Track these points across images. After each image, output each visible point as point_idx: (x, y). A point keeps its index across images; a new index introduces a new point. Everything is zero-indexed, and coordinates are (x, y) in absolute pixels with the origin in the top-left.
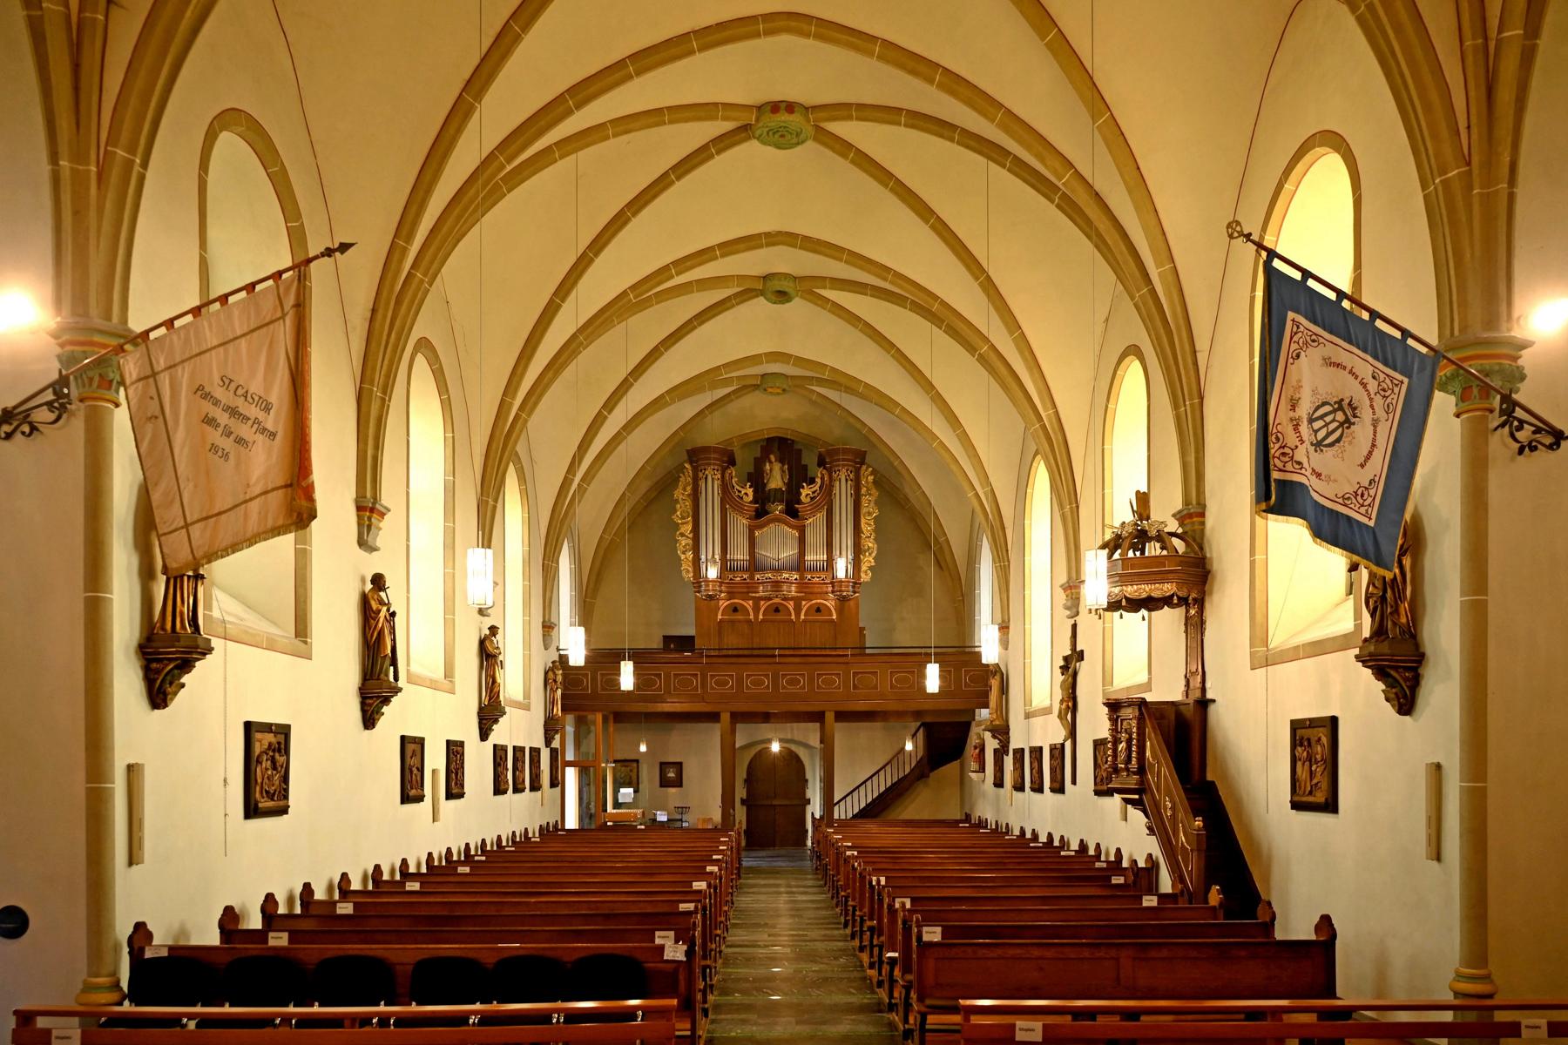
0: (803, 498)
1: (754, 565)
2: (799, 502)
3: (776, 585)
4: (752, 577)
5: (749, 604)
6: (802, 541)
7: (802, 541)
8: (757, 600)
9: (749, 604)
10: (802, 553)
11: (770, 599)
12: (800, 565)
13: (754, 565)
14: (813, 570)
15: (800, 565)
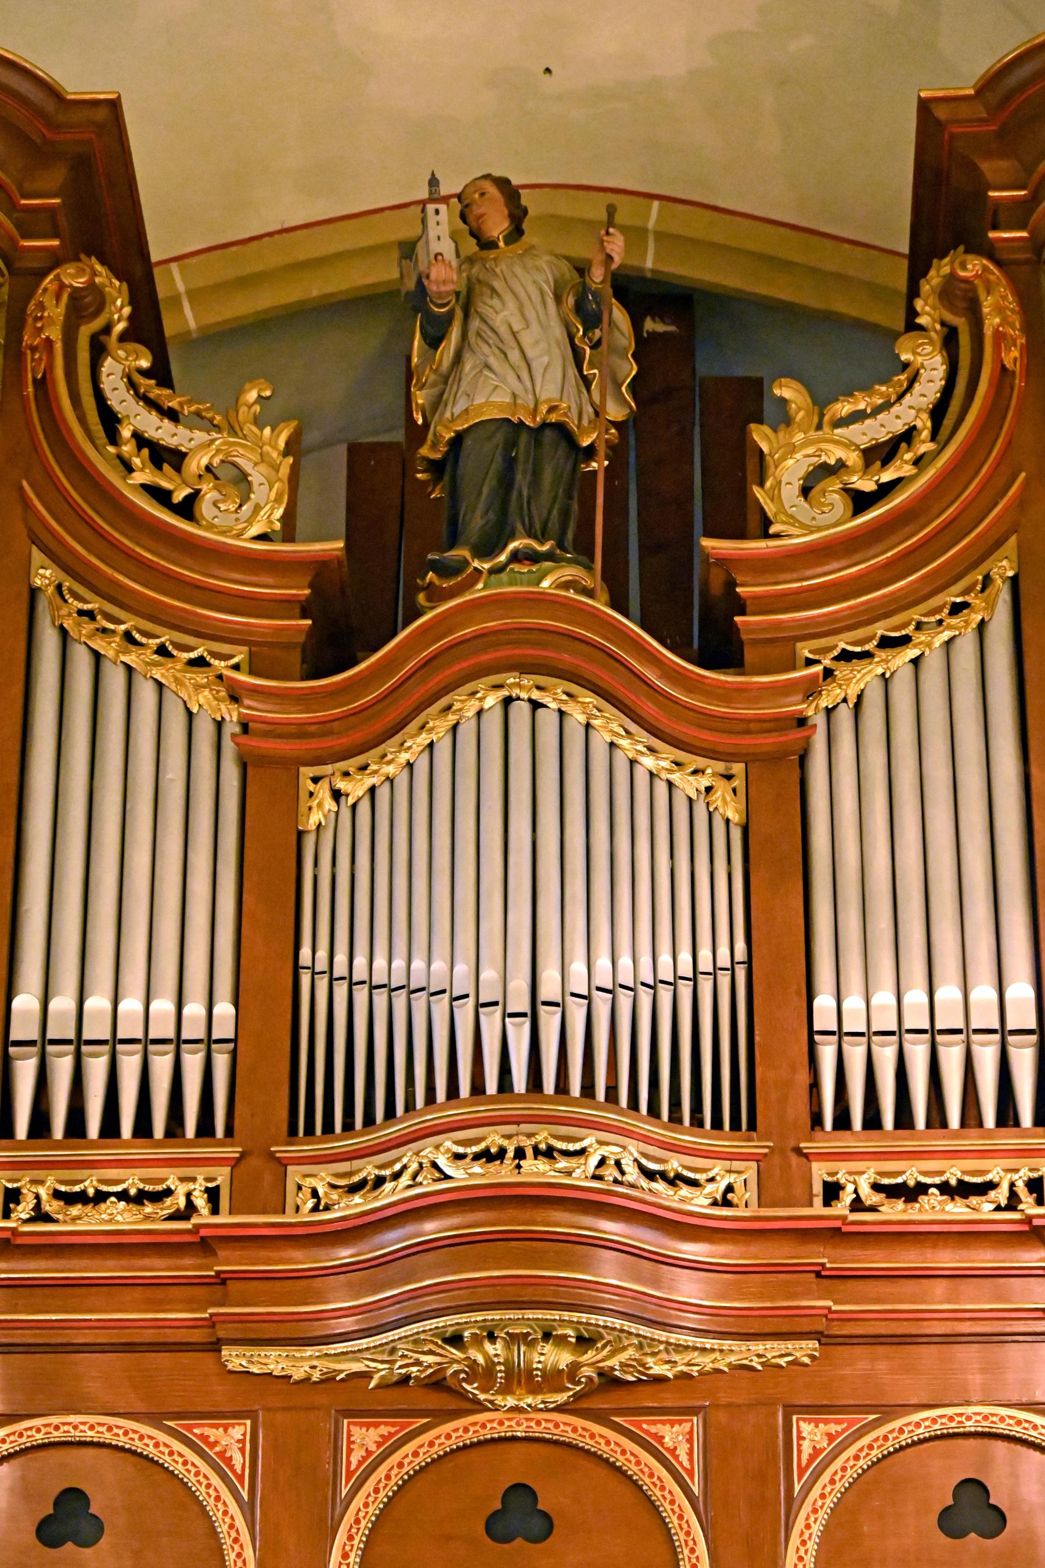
0: (780, 490)
1: (295, 1079)
2: (744, 519)
3: (520, 1233)
4: (260, 1180)
5: (213, 1464)
6: (776, 861)
7: (776, 861)
8: (301, 1428)
9: (213, 1464)
10: (780, 954)
11: (444, 1395)
12: (749, 1072)
13: (295, 1079)
14: (892, 1112)
15: (749, 1072)
